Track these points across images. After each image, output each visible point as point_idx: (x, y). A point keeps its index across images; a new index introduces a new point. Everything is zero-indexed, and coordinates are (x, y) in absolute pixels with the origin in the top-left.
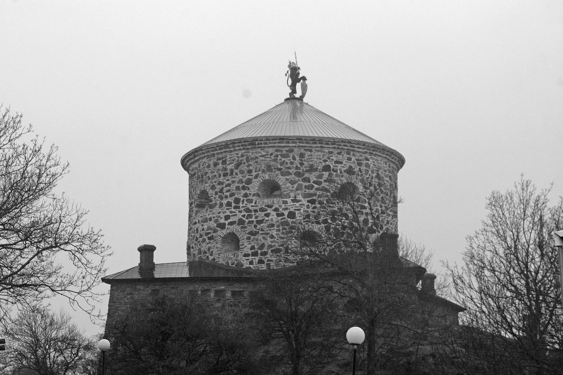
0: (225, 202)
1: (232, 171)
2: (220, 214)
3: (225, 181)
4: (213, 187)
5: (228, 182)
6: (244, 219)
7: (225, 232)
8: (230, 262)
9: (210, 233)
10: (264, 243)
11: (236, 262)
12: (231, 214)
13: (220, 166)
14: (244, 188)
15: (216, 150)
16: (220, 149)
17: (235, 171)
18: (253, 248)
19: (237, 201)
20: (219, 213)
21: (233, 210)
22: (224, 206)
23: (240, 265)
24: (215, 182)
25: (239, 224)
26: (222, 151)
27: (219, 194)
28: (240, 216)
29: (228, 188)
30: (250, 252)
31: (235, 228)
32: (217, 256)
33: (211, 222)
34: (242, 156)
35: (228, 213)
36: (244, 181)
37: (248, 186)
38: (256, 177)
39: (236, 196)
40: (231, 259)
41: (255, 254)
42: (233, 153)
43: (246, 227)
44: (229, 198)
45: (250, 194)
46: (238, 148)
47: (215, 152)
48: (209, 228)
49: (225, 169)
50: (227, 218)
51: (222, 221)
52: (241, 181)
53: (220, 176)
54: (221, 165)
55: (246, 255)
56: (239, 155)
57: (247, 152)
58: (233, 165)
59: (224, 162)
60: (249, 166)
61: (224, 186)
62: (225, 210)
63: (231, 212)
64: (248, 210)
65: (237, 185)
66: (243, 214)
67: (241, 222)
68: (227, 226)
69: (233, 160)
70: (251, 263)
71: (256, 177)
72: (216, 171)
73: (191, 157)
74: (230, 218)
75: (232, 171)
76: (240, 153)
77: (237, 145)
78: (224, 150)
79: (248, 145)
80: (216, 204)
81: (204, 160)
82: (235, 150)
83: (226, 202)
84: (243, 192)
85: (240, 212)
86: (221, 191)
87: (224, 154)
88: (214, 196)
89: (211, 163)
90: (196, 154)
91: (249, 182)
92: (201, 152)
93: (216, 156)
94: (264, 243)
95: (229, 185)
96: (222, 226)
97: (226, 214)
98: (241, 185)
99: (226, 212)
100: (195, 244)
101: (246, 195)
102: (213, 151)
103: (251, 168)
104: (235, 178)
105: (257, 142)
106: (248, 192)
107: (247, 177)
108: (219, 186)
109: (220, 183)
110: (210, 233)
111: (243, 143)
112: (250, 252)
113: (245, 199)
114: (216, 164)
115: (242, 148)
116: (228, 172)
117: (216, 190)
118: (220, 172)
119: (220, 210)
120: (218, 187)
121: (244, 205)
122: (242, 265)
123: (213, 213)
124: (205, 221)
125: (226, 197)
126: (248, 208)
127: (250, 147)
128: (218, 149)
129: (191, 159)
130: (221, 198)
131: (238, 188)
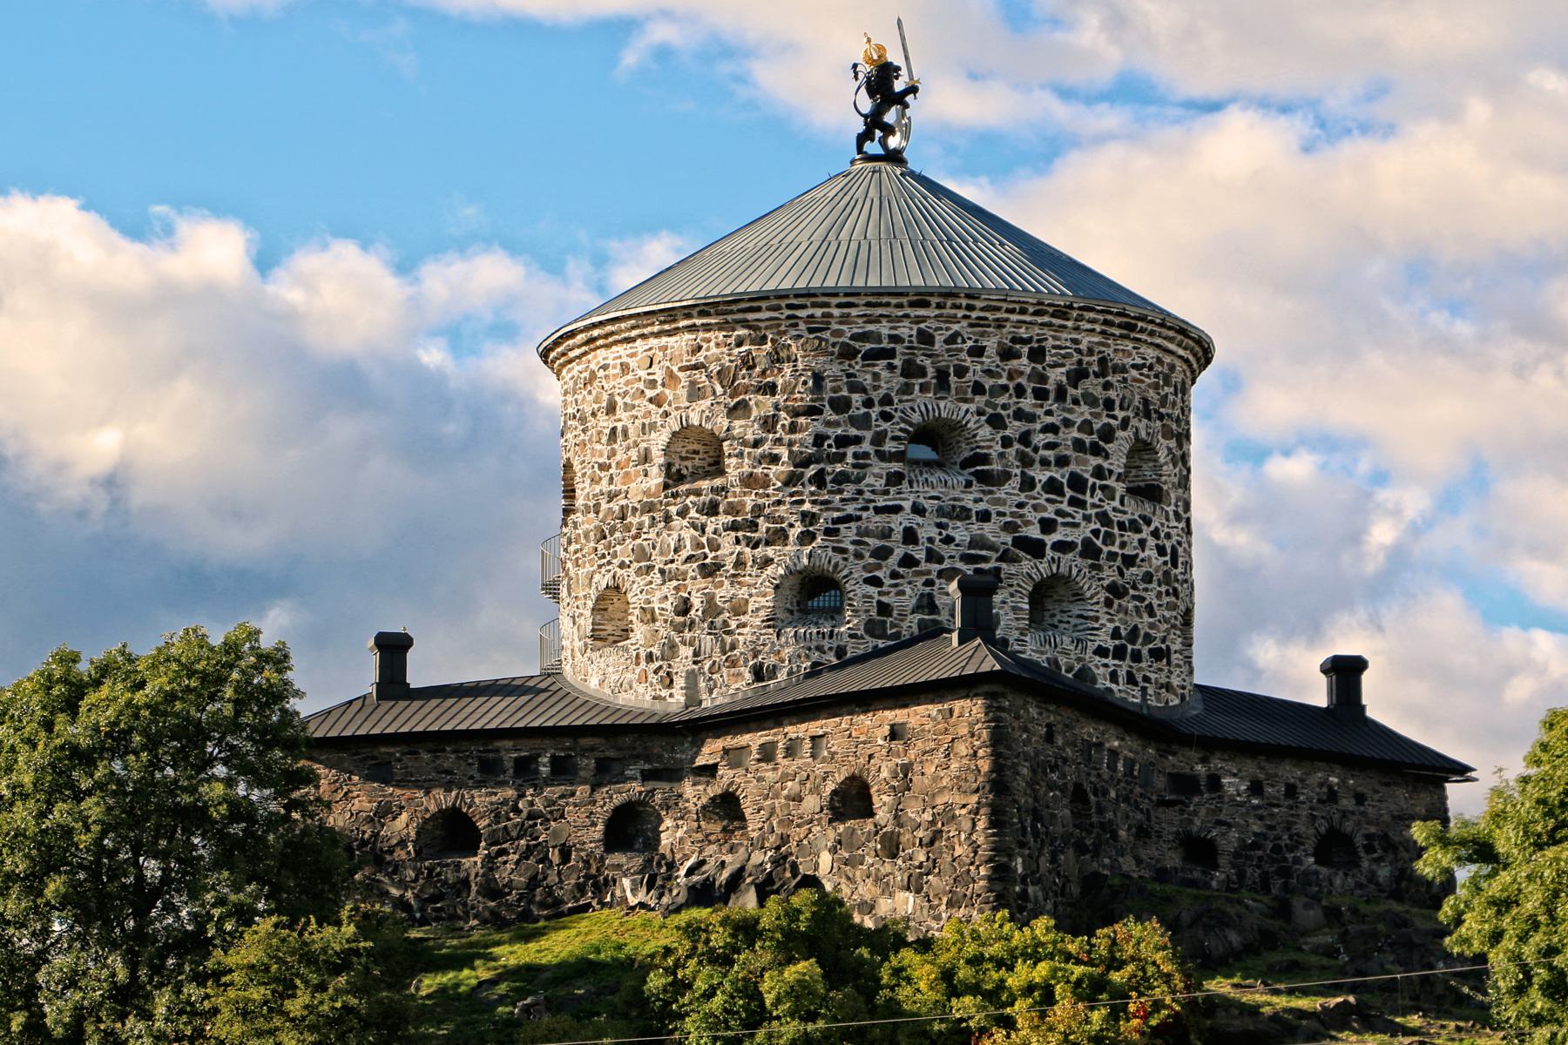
0: (1041, 476)
1: (1061, 394)
2: (1024, 511)
3: (1040, 412)
4: (996, 422)
5: (1049, 420)
6: (1099, 543)
7: (1044, 567)
8: (1062, 660)
9: (985, 559)
10: (1136, 627)
11: (1077, 667)
12: (1060, 520)
13: (1023, 364)
14: (1096, 450)
15: (1023, 311)
16: (1036, 313)
17: (1071, 391)
18: (1116, 634)
19: (1077, 482)
20: (1021, 505)
21: (1065, 507)
22: (1039, 487)
23: (1084, 674)
24: (1004, 407)
25: (1083, 555)
26: (1039, 320)
27: (1017, 446)
28: (1086, 530)
29: (1050, 437)
30: (1111, 644)
31: (1071, 563)
32: (1016, 634)
33: (987, 527)
34: (1091, 352)
35: (1049, 514)
36: (1096, 427)
37: (1107, 447)
38: (1125, 424)
39: (1073, 467)
40: (1065, 653)
41: (1119, 653)
42: (1064, 335)
43: (1099, 568)
44: (1053, 467)
45: (1111, 472)
46: (1089, 326)
47: (1014, 317)
48: (977, 542)
49: (1043, 379)
50: (1048, 526)
51: (1034, 532)
52: (1086, 427)
53: (1020, 392)
54: (1024, 360)
55: (1101, 652)
56: (1083, 347)
57: (1103, 344)
58: (1063, 370)
59: (1037, 355)
60: (1107, 386)
61: (1038, 426)
62: (1042, 501)
63: (1059, 513)
64: (1104, 518)
65: (1076, 434)
66: (1093, 526)
67: (1090, 550)
68: (1049, 553)
69: (1064, 357)
70: (1114, 677)
71: (1125, 424)
72: (1005, 375)
73: (894, 301)
74: (1054, 530)
75: (1061, 394)
76: (1086, 341)
77: (1092, 315)
78: (1046, 319)
79: (1120, 326)
80: (1007, 476)
81: (955, 327)
82: (1077, 329)
83: (1044, 479)
84: (1095, 461)
85: (1087, 518)
86: (1025, 438)
87: (1037, 330)
88: (999, 448)
89: (991, 344)
90: (934, 300)
91: (1108, 434)
92: (964, 302)
93: (1008, 328)
94: (1136, 627)
95: (1051, 429)
96: (1035, 549)
97: (1046, 515)
98: (1087, 439)
99: (1045, 509)
100: (894, 575)
101: (1099, 472)
102: (1012, 311)
103: (1112, 394)
104: (1070, 411)
105: (1140, 324)
106: (1106, 465)
107: (1106, 420)
108: (1017, 423)
109: (1020, 415)
110: (985, 559)
111: (1109, 317)
112: (1111, 644)
113: (1098, 482)
114: (1007, 354)
115: (1098, 328)
116: (1051, 386)
117: (1007, 432)
118: (1022, 380)
119: (1022, 498)
120: (1014, 428)
121: (1096, 500)
122: (1094, 680)
123: (998, 502)
124: (964, 514)
125: (1045, 463)
126: (1105, 514)
127: (1117, 332)
128: (1031, 310)
129: (888, 305)
130: (1026, 462)
131: (1079, 445)
